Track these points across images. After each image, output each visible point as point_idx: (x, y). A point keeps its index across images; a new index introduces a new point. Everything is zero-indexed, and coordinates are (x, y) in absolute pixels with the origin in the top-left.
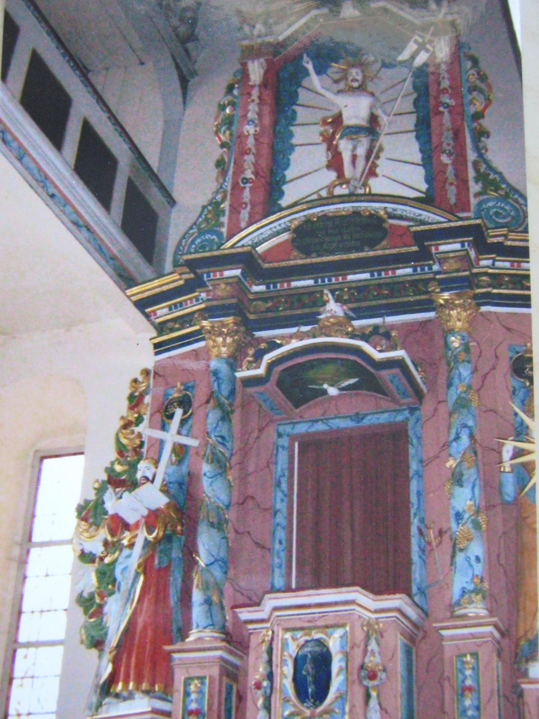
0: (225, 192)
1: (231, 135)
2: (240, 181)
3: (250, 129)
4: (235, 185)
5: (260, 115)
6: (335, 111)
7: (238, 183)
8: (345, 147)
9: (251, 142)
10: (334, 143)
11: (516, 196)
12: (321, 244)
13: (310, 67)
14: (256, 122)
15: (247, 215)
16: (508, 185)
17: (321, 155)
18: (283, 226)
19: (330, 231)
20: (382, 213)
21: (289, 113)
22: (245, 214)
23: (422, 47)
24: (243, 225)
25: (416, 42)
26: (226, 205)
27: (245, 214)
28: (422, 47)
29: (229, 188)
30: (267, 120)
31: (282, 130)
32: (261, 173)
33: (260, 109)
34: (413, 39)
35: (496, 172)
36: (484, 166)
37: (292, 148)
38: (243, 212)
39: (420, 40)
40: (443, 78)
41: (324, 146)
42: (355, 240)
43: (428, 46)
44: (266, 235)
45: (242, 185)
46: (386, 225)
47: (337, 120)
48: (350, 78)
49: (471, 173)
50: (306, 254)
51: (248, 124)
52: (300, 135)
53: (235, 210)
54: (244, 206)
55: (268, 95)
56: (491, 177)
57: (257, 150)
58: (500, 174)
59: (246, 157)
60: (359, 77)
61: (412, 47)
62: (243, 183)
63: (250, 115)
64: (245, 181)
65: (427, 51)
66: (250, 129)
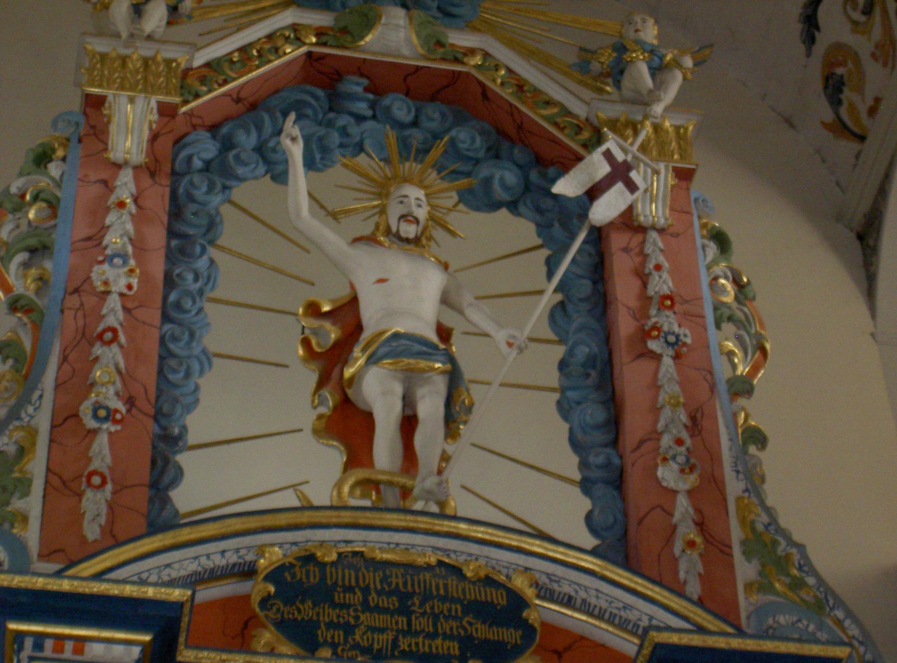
0: (33, 433)
1: (42, 280)
2: (85, 409)
3: (117, 278)
4: (65, 420)
5: (138, 243)
6: (343, 293)
7: (76, 415)
8: (378, 391)
9: (113, 313)
10: (348, 372)
11: (840, 614)
12: (349, 629)
13: (296, 151)
14: (132, 262)
15: (104, 510)
16: (820, 580)
17: (297, 397)
18: (232, 558)
19: (373, 598)
20: (520, 583)
21: (202, 264)
22: (94, 504)
23: (620, 173)
24: (92, 532)
25: (608, 155)
26: (37, 466)
27: (94, 504)
28: (620, 173)
29: (43, 422)
30: (158, 267)
31: (188, 304)
32: (141, 402)
33: (138, 231)
34: (603, 148)
35: (792, 543)
36: (765, 518)
37: (207, 358)
38: (89, 494)
39: (620, 157)
40: (658, 267)
41: (311, 377)
42: (445, 637)
43: (633, 175)
44: (183, 573)
45: (92, 424)
46: (532, 616)
47: (348, 312)
48: (394, 212)
49: (736, 534)
50: (307, 650)
51: (110, 259)
52: (221, 329)
53: (64, 486)
54: (96, 480)
55: (158, 198)
56: (780, 550)
57: (131, 339)
58: (801, 547)
59: (98, 350)
60: (422, 214)
61: (596, 166)
62: (95, 416)
63: (114, 240)
64: (102, 413)
65: (632, 187)
66: (117, 278)
